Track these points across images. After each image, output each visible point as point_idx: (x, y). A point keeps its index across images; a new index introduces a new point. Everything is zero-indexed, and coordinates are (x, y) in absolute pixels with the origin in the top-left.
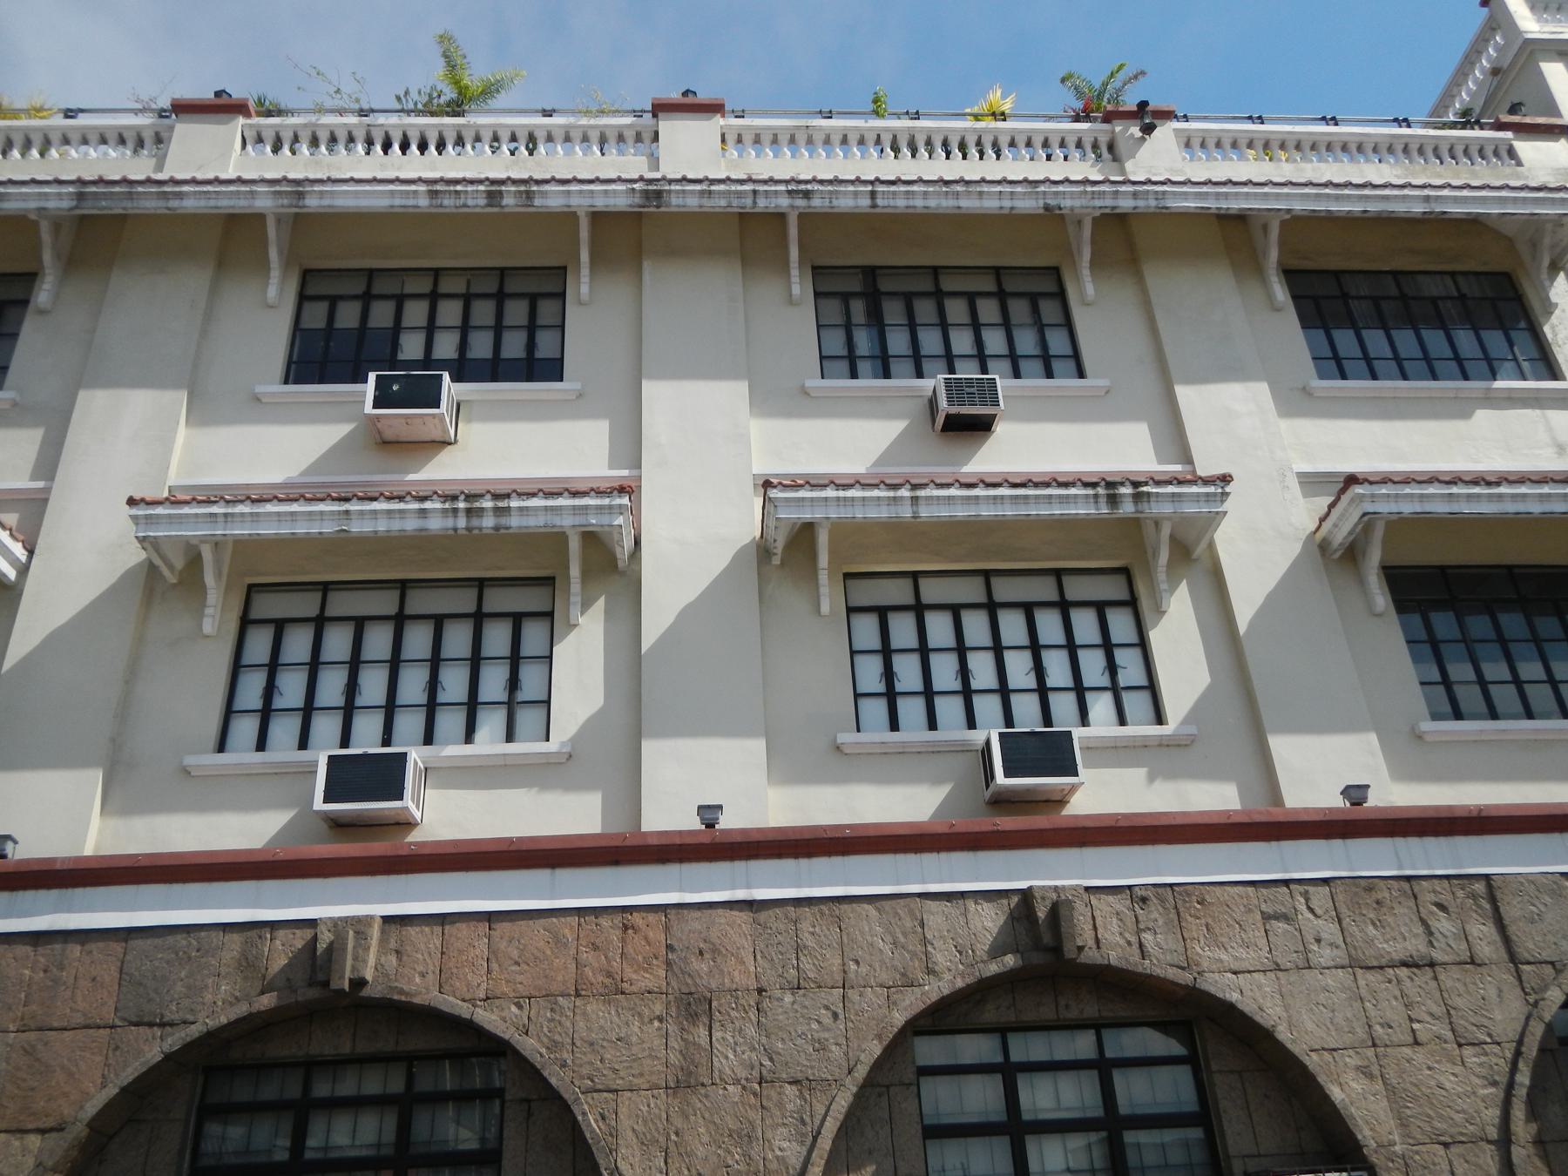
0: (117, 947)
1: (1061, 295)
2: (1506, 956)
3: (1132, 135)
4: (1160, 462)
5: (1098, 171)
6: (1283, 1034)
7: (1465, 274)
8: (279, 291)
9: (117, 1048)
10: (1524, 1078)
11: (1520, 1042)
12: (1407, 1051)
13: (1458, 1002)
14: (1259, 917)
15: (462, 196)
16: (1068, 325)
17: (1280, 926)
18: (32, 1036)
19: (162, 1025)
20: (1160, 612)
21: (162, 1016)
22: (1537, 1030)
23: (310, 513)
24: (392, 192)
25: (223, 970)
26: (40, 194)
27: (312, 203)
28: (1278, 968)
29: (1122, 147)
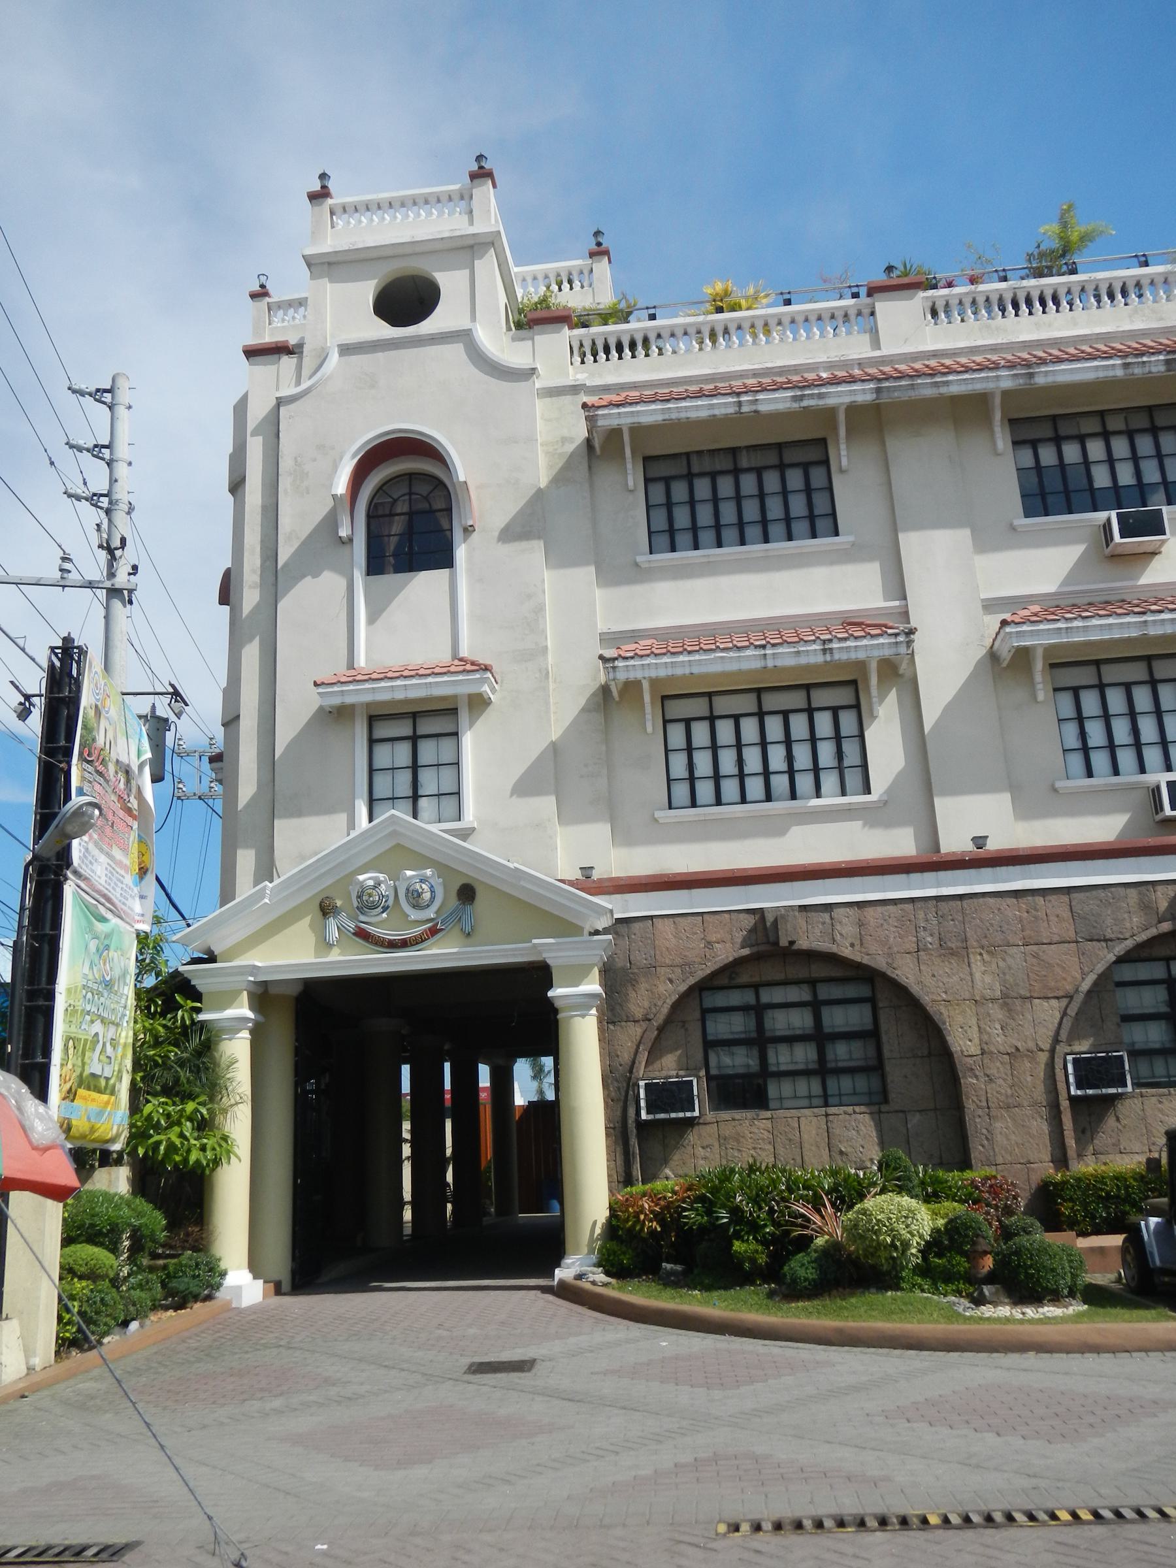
0: (1065, 898)
8: (1002, 439)
9: (1083, 954)
15: (1147, 365)
18: (1035, 948)
19: (1106, 940)
21: (1105, 936)
23: (1122, 624)
24: (1097, 367)
25: (1131, 909)
26: (850, 391)
27: (1040, 380)
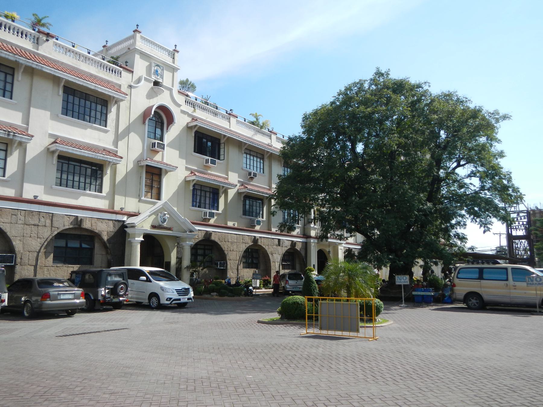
1: (13, 75)
2: (51, 226)
3: (43, 39)
4: (22, 123)
5: (33, 45)
6: (8, 234)
7: (99, 98)
10: (46, 244)
11: (47, 239)
12: (28, 238)
13: (40, 232)
14: (11, 214)
16: (12, 84)
17: (14, 216)
20: (11, 154)
22: (51, 237)
28: (11, 223)
29: (40, 41)
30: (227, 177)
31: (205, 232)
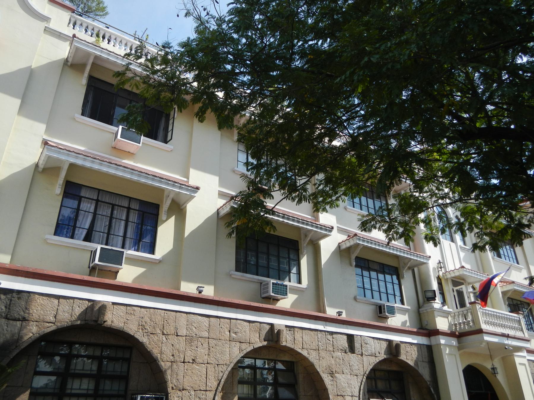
30: (186, 179)
31: (87, 304)
